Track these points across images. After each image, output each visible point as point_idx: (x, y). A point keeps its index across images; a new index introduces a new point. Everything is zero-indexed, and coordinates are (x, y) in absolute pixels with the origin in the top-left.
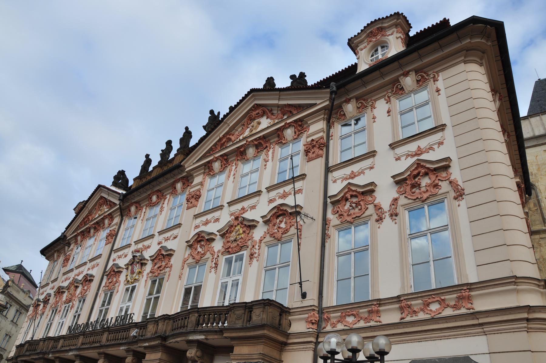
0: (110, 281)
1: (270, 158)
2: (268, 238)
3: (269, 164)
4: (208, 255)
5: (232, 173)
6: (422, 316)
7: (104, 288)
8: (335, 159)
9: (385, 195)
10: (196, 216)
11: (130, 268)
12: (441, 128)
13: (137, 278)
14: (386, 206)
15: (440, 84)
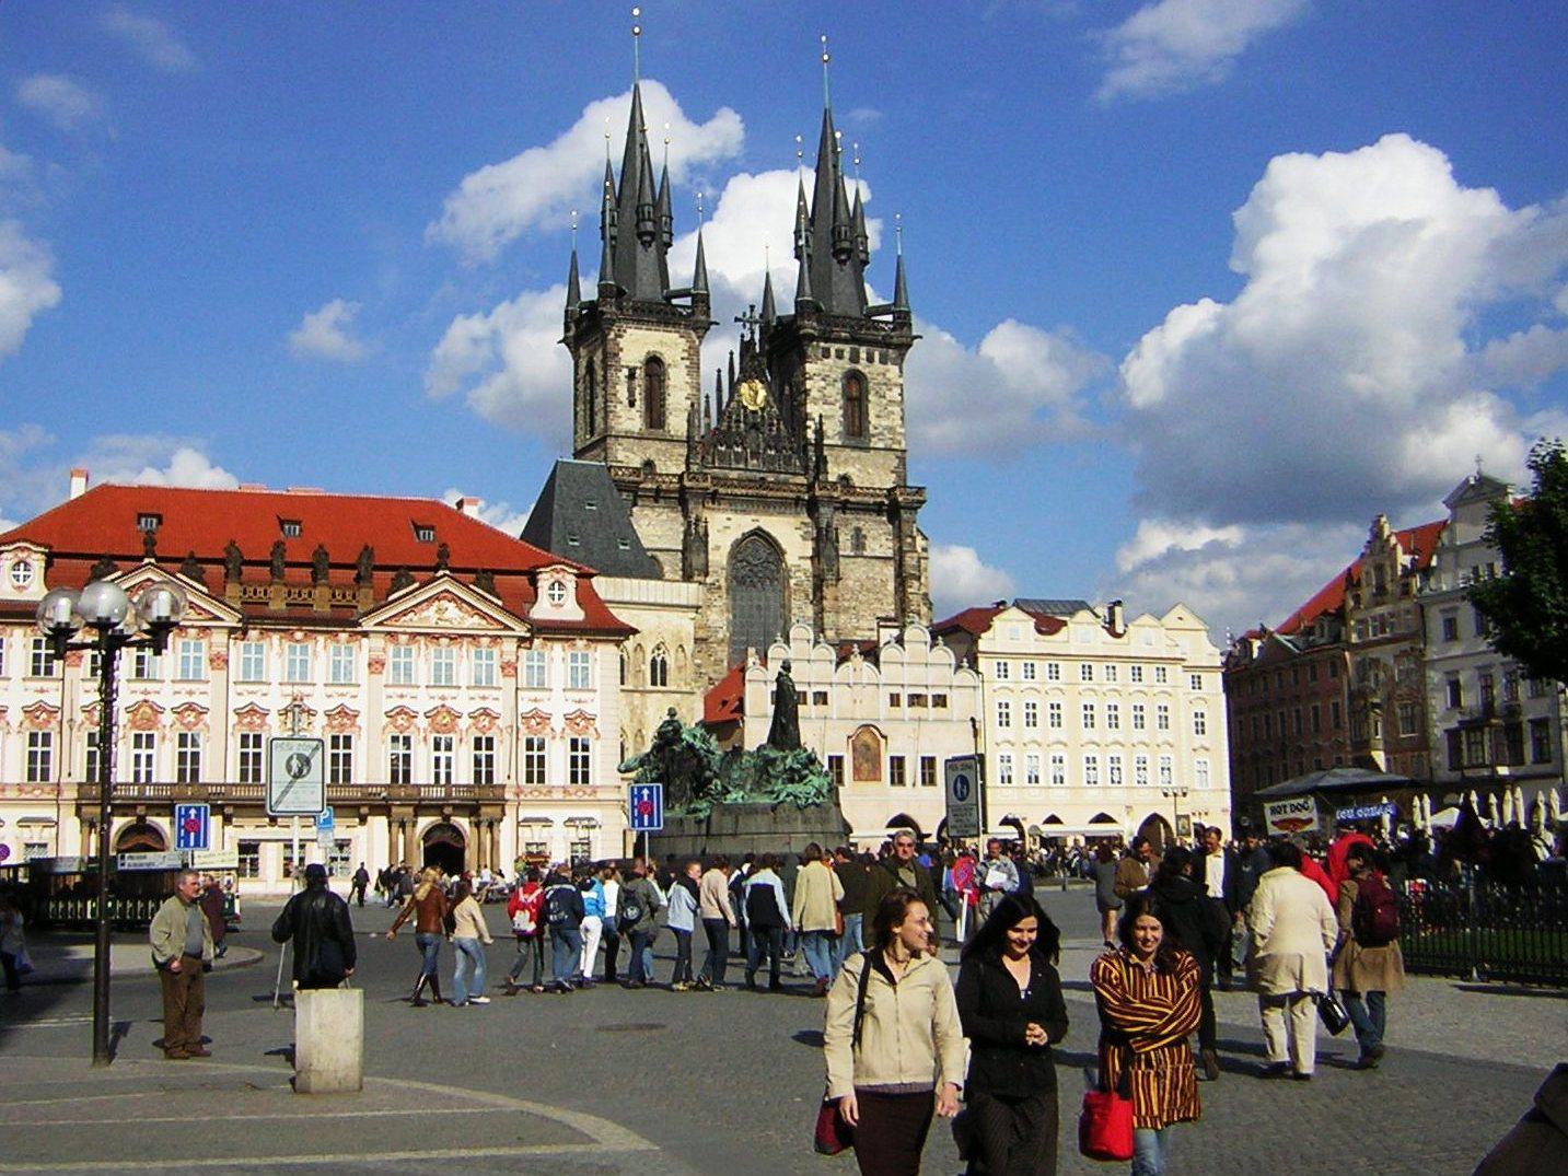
0: (248, 719)
1: (465, 654)
2: (473, 729)
3: (465, 659)
4: (412, 728)
5: (422, 654)
6: (574, 797)
7: (238, 727)
8: (523, 683)
9: (558, 723)
10: (386, 686)
11: (290, 714)
12: (595, 691)
13: (305, 726)
14: (558, 730)
15: (597, 655)
